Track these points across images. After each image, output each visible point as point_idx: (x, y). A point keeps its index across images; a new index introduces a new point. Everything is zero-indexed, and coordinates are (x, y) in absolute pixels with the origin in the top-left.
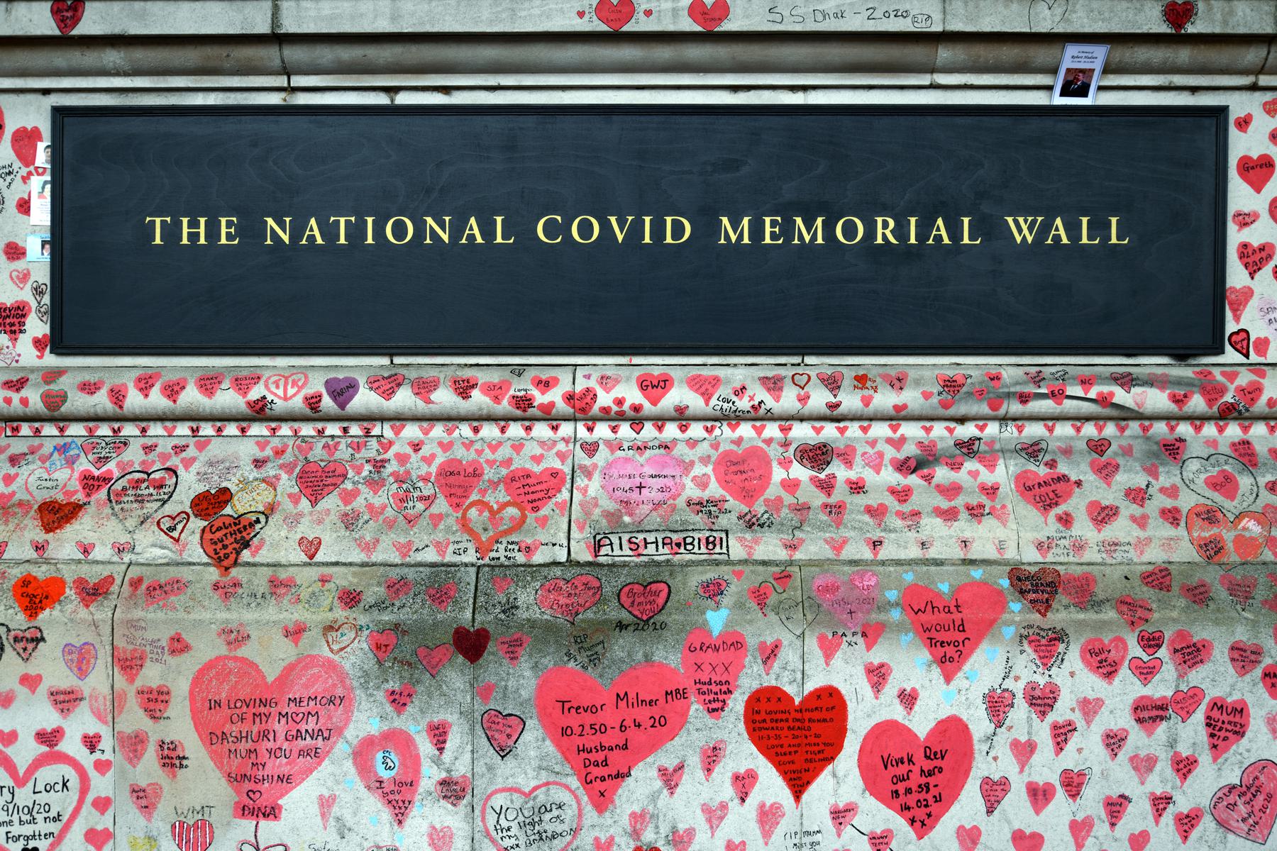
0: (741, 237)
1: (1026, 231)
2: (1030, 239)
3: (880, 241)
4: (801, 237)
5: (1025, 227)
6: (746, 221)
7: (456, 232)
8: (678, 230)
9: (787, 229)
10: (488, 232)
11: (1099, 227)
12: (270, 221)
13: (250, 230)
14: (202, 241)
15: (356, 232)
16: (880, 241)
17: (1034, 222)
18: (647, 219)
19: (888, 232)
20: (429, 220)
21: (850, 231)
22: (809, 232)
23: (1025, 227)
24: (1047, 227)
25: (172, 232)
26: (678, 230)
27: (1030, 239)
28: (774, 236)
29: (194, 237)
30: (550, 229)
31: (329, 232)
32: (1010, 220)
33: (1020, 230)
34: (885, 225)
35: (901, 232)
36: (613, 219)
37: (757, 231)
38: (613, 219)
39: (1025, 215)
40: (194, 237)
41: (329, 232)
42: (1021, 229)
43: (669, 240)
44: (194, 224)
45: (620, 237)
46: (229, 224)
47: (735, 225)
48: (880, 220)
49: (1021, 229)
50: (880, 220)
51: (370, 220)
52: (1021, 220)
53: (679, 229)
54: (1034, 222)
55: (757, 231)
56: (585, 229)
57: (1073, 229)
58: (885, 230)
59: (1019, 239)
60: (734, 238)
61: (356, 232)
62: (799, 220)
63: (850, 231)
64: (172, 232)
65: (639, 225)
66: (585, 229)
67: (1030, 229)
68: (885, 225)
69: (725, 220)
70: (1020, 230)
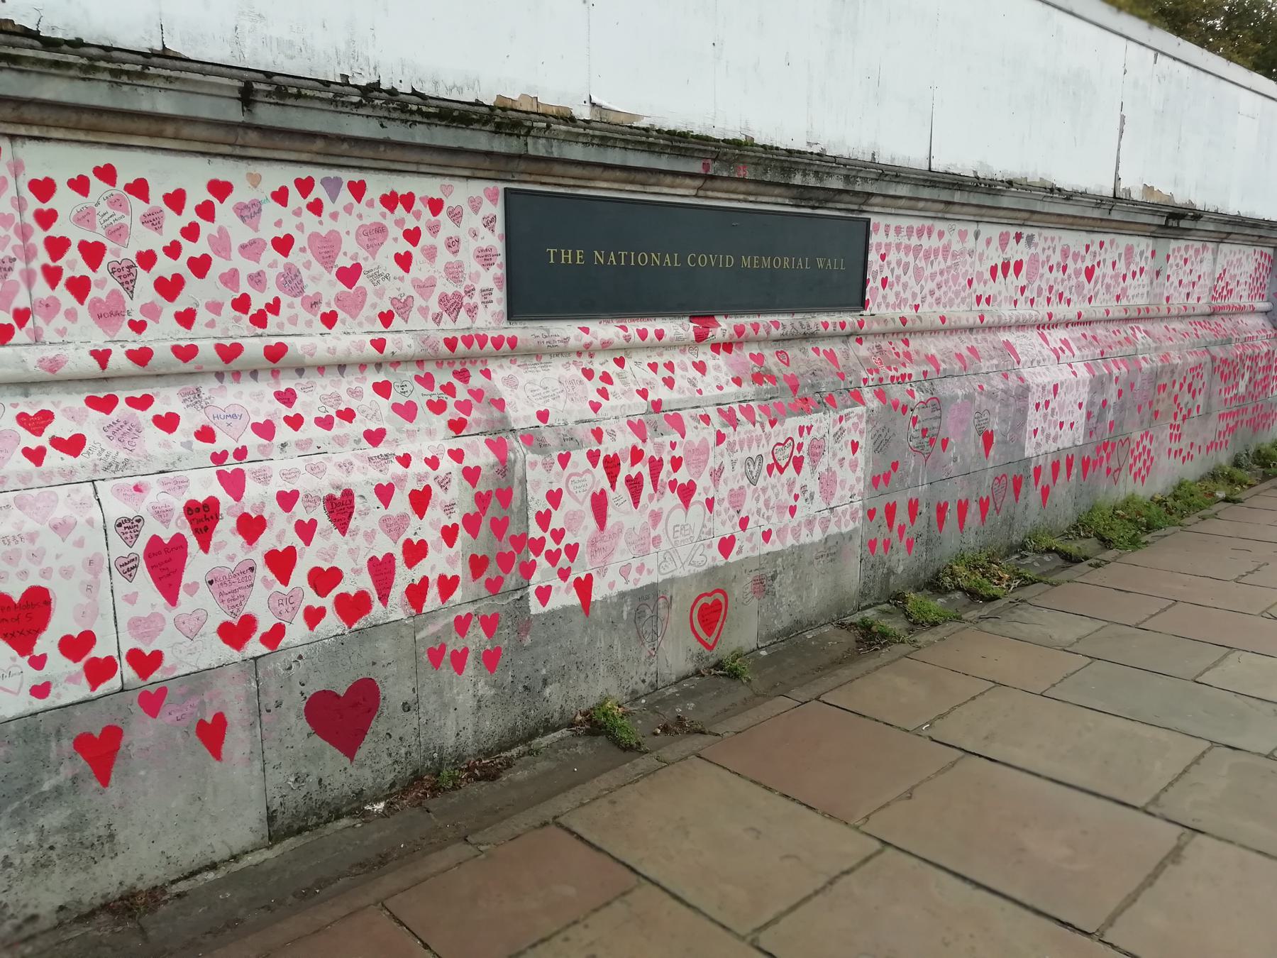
9: (760, 263)
10: (673, 262)
13: (589, 257)
15: (628, 258)
22: (766, 263)
25: (557, 256)
29: (566, 259)
40: (566, 259)
41: (618, 258)
44: (566, 253)
61: (628, 258)
64: (557, 256)
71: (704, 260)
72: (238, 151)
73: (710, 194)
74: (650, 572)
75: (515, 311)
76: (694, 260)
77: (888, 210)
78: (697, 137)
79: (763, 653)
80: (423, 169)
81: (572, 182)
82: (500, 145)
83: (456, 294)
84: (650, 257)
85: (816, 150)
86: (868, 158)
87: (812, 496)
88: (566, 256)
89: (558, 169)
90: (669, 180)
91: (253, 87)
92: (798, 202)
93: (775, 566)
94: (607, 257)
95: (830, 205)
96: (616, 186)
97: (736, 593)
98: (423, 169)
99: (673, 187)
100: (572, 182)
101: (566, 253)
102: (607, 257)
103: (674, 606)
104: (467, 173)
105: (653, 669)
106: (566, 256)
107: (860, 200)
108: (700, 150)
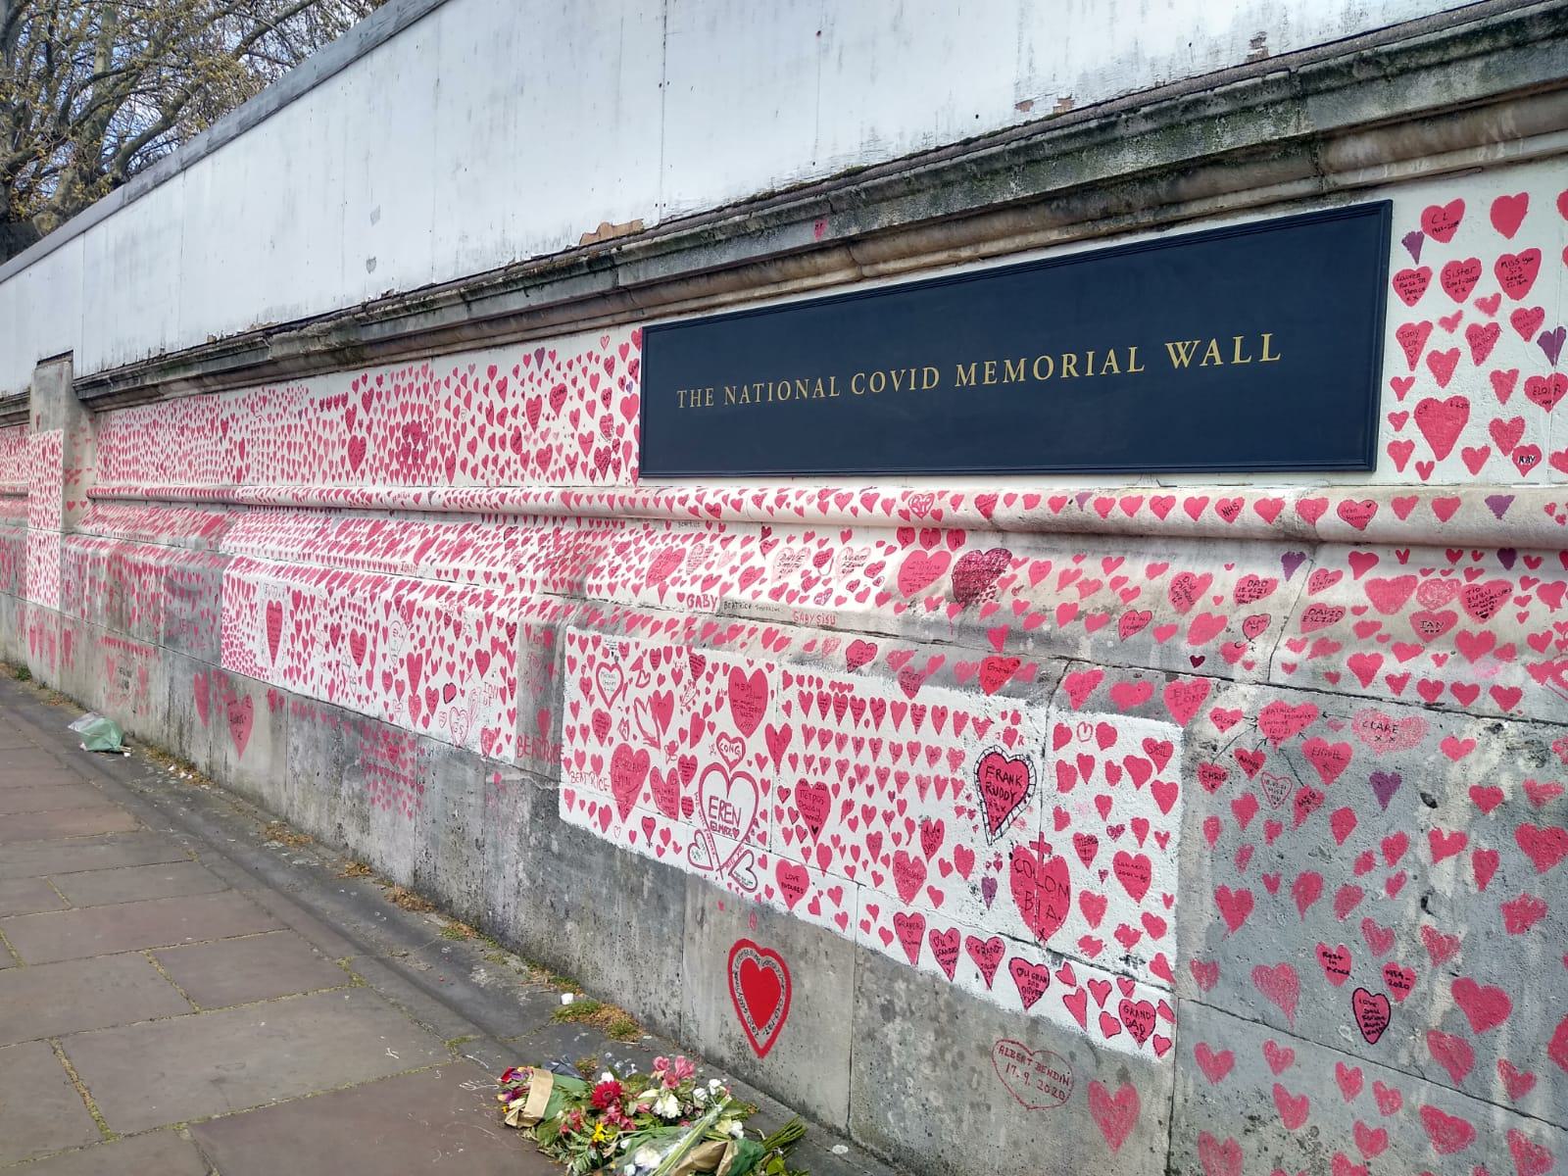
1: (1183, 356)
3: (1065, 375)
6: (973, 368)
9: (1000, 371)
10: (827, 390)
13: (719, 397)
15: (764, 392)
16: (1065, 375)
17: (1192, 345)
18: (913, 371)
19: (1071, 367)
21: (1044, 368)
24: (1204, 347)
28: (991, 378)
32: (1170, 346)
34: (1070, 361)
35: (1081, 366)
39: (1183, 340)
42: (1179, 354)
43: (925, 387)
48: (1065, 356)
49: (1179, 354)
50: (1065, 356)
52: (1179, 344)
54: (1192, 345)
57: (1227, 352)
58: (1069, 368)
59: (1176, 364)
61: (764, 392)
63: (1044, 368)
67: (1187, 354)
68: (1070, 361)
71: (879, 382)
72: (487, 342)
73: (882, 267)
74: (677, 849)
75: (652, 466)
76: (861, 384)
77: (1480, 156)
78: (788, 191)
79: (840, 1149)
80: (582, 325)
81: (694, 304)
82: (601, 283)
83: (607, 449)
85: (1038, 112)
86: (1232, 56)
87: (989, 888)
89: (667, 293)
90: (791, 266)
91: (472, 290)
92: (1088, 228)
93: (890, 990)
95: (1195, 208)
96: (742, 295)
97: (808, 984)
98: (582, 325)
99: (818, 274)
100: (694, 304)
103: (706, 927)
104: (607, 321)
105: (675, 1005)
107: (1300, 163)
108: (798, 209)
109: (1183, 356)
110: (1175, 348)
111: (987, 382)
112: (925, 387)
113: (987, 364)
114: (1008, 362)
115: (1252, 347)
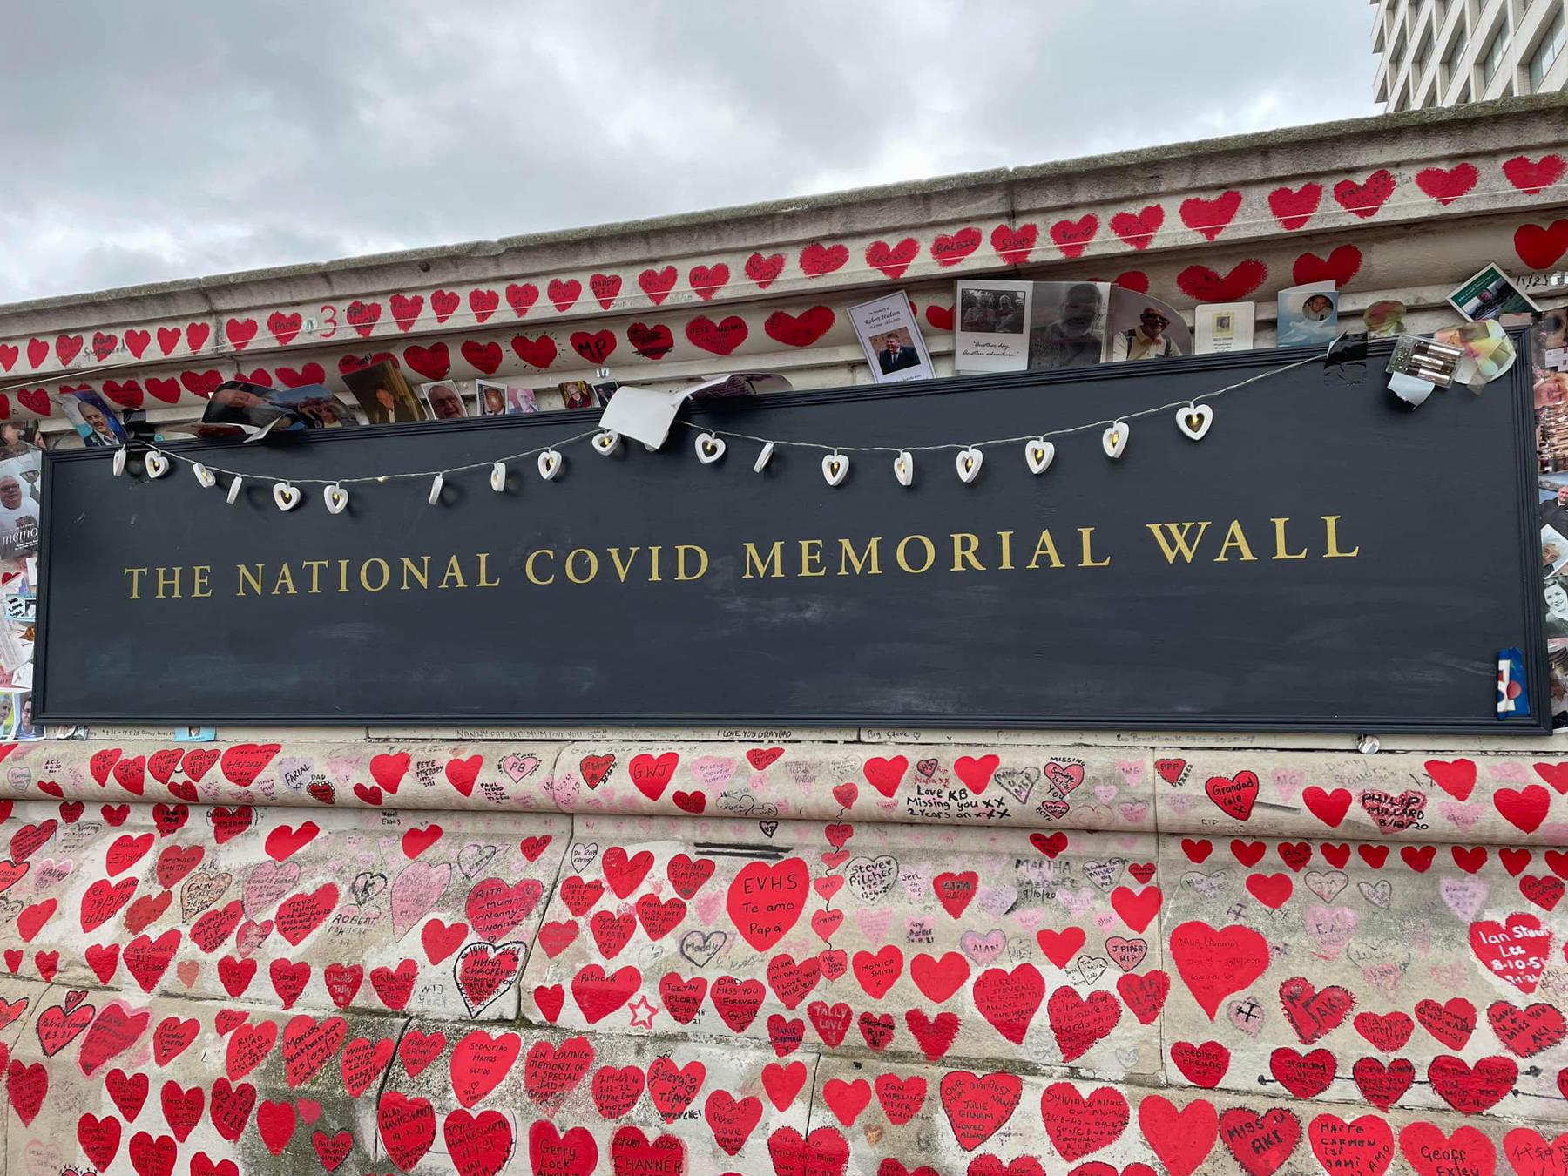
0: (771, 569)
1: (1181, 544)
2: (1189, 556)
3: (958, 567)
4: (849, 566)
5: (1180, 540)
7: (436, 573)
8: (692, 561)
9: (831, 556)
10: (471, 573)
11: (1306, 534)
12: (243, 569)
13: (224, 579)
14: (177, 594)
15: (329, 577)
16: (958, 567)
18: (655, 550)
20: (406, 561)
23: (1180, 540)
25: (148, 583)
26: (692, 561)
27: (1189, 556)
28: (813, 566)
29: (169, 589)
30: (541, 568)
31: (302, 578)
32: (1155, 529)
33: (1172, 544)
34: (966, 545)
35: (989, 553)
36: (614, 552)
37: (791, 559)
38: (614, 552)
40: (169, 589)
41: (302, 578)
43: (681, 576)
44: (169, 575)
45: (623, 575)
46: (203, 574)
47: (764, 553)
48: (957, 538)
51: (344, 563)
52: (1173, 527)
53: (693, 562)
55: (791, 559)
56: (581, 567)
57: (1261, 539)
60: (762, 570)
61: (329, 577)
62: (846, 544)
64: (148, 583)
65: (644, 556)
66: (581, 567)
67: (1189, 541)
68: (966, 545)
69: (751, 547)
70: (1172, 544)
84: (397, 570)
88: (168, 583)
94: (270, 579)
101: (169, 575)
102: (270, 579)
106: (168, 583)
109: (1181, 544)
110: (1166, 533)
111: (806, 572)
112: (681, 576)
113: (805, 544)
114: (846, 544)
115: (1306, 534)
